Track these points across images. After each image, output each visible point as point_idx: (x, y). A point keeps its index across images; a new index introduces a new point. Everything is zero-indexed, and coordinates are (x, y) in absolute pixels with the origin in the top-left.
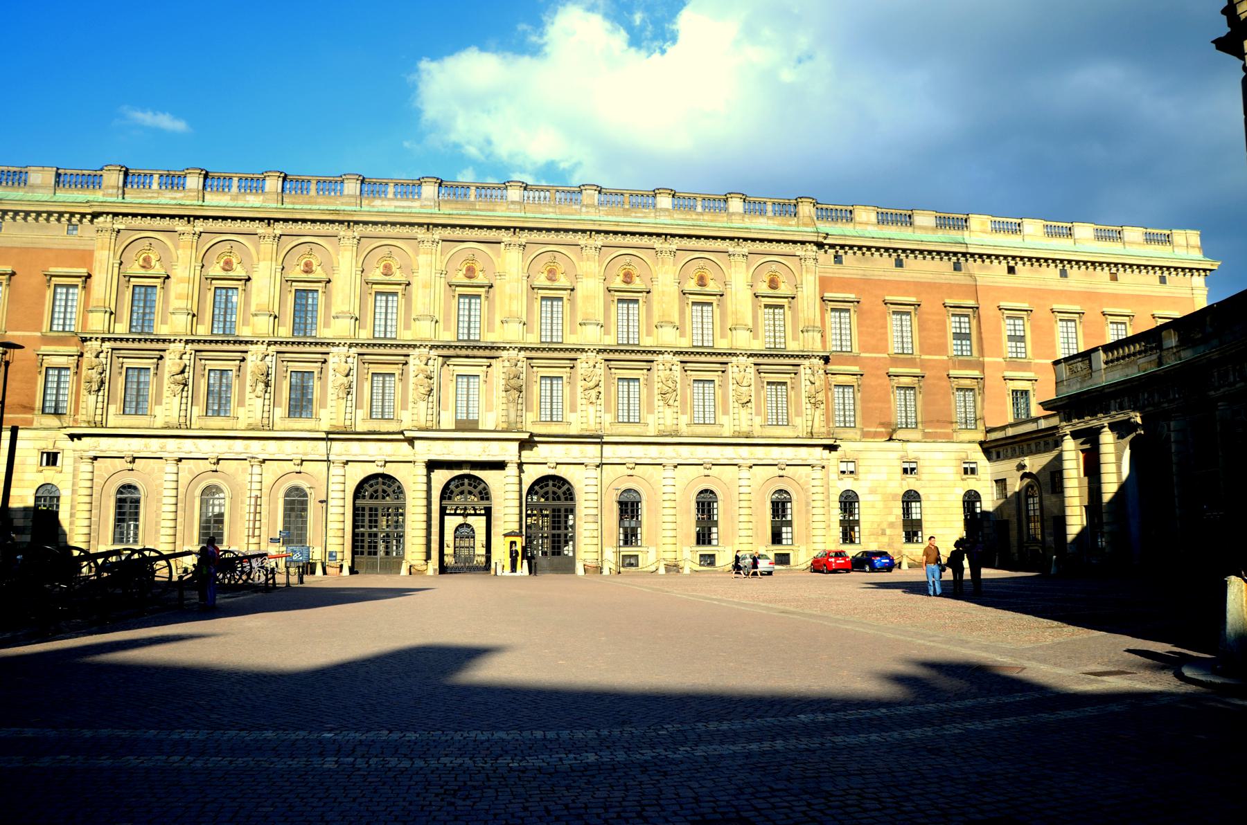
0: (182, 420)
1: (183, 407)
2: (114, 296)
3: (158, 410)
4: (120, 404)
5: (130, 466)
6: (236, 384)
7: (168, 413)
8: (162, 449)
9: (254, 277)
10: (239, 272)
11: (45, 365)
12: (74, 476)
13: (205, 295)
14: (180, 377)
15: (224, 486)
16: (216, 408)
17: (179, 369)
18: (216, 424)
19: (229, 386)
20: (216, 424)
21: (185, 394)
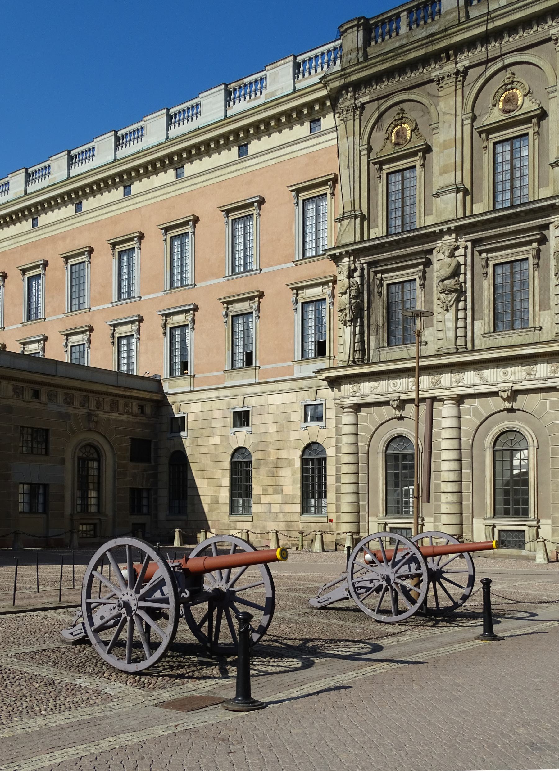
0: (460, 342)
1: (461, 323)
2: (364, 194)
3: (429, 334)
4: (383, 334)
5: (398, 413)
6: (533, 275)
7: (441, 335)
8: (436, 385)
9: (552, 108)
10: (528, 106)
11: (301, 301)
12: (338, 431)
13: (481, 159)
14: (450, 283)
15: (527, 431)
16: (508, 318)
17: (447, 271)
18: (511, 340)
19: (524, 283)
20: (511, 340)
21: (461, 305)
